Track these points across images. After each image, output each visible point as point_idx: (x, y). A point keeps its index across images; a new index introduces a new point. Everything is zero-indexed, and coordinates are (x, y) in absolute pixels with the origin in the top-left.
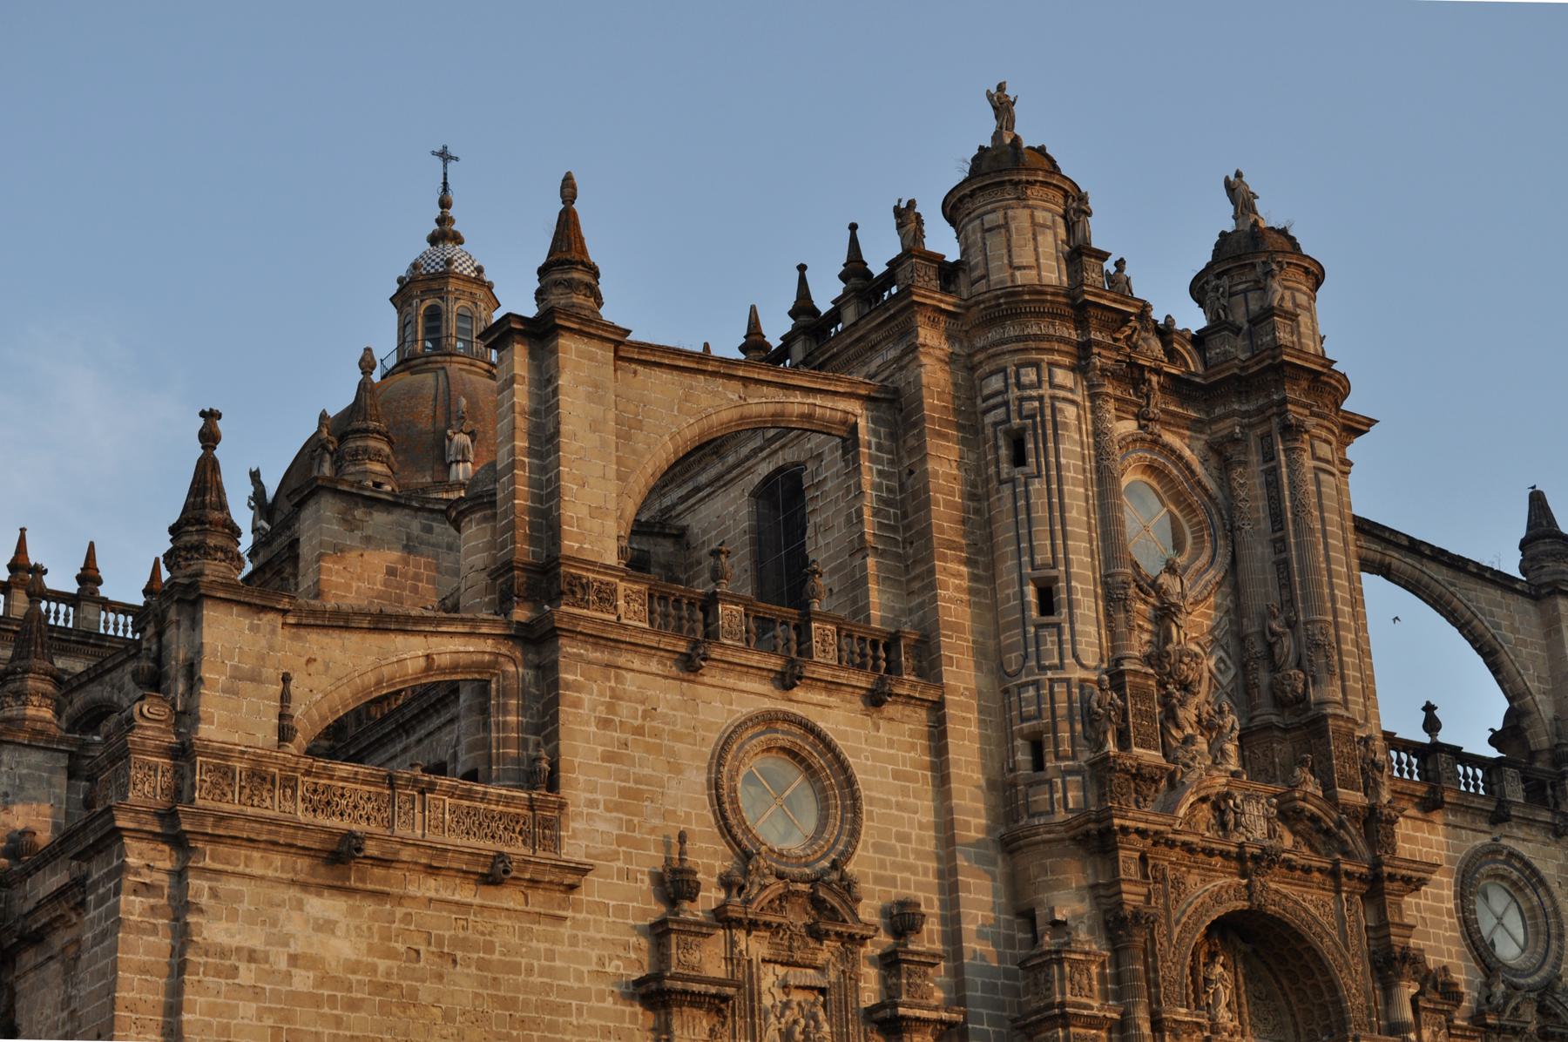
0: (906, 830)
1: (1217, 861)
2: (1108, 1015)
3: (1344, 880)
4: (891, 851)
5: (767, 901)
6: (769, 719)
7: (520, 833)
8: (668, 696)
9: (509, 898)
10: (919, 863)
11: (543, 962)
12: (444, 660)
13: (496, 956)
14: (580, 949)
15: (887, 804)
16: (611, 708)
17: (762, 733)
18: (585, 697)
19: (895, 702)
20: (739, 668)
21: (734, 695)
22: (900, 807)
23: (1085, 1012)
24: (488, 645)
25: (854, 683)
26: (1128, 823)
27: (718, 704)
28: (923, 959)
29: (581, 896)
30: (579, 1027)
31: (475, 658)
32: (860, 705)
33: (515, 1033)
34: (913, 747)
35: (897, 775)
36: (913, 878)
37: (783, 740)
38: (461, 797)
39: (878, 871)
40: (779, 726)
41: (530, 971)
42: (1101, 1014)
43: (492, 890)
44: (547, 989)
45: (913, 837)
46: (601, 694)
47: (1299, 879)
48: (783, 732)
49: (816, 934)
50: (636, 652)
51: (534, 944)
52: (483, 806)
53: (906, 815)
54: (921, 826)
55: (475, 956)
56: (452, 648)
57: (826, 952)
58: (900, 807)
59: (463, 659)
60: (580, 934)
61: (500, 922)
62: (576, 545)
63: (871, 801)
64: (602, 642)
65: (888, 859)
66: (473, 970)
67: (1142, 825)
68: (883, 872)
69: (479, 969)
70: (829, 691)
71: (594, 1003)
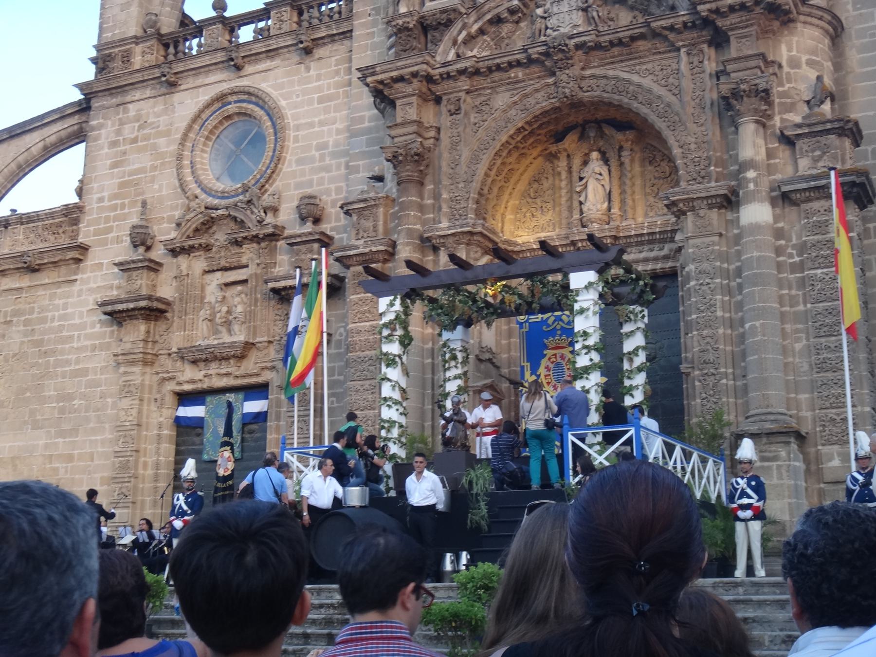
0: (325, 139)
1: (520, 73)
2: (374, 249)
3: (672, 36)
4: (312, 160)
5: (191, 229)
6: (221, 99)
7: (63, 232)
8: (156, 110)
9: (44, 278)
10: (333, 162)
11: (62, 312)
12: (53, 139)
13: (35, 315)
14: (83, 298)
15: (311, 125)
16: (118, 132)
17: (220, 108)
18: (103, 131)
19: (325, 44)
20: (202, 70)
21: (201, 90)
22: (322, 123)
23: (352, 253)
24: (75, 120)
25: (283, 45)
26: (380, 77)
27: (189, 101)
28: (304, 239)
29: (90, 261)
30: (77, 349)
31: (70, 130)
32: (295, 57)
33: (40, 361)
34: (337, 73)
35: (321, 101)
36: (327, 175)
37: (232, 108)
38: (28, 223)
39: (298, 180)
40: (231, 99)
41: (53, 319)
42: (367, 250)
43: (37, 275)
44: (61, 328)
45: (331, 143)
46: (113, 125)
47: (621, 55)
48: (235, 102)
49: (237, 243)
50: (136, 88)
51: (57, 302)
52: (39, 224)
53: (325, 128)
54: (338, 132)
55: (23, 318)
56: (55, 130)
57: (248, 253)
58: (322, 123)
59: (63, 134)
60: (84, 287)
61: (39, 293)
62: (110, 34)
63: (297, 128)
64: (114, 91)
65: (307, 167)
66: (22, 328)
67: (394, 74)
68: (304, 179)
69: (24, 326)
70: (272, 58)
71: (89, 331)
